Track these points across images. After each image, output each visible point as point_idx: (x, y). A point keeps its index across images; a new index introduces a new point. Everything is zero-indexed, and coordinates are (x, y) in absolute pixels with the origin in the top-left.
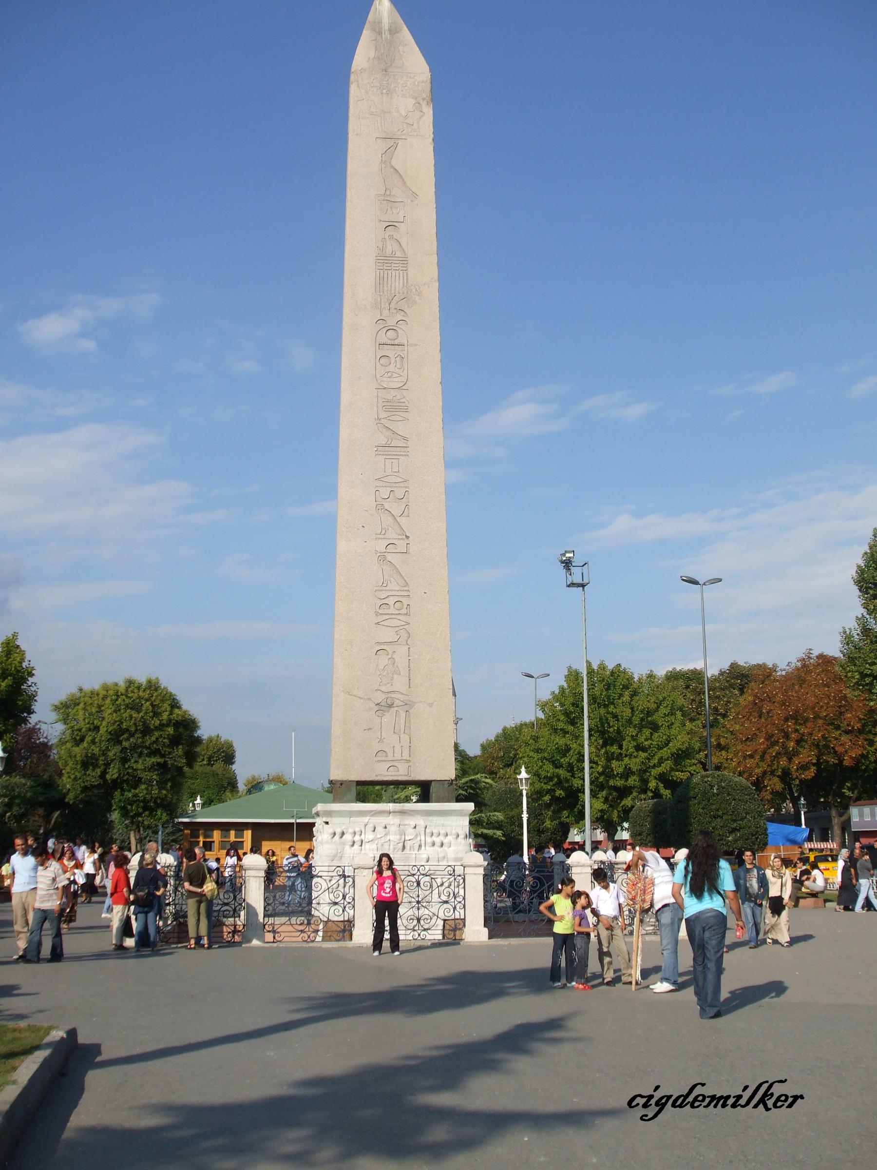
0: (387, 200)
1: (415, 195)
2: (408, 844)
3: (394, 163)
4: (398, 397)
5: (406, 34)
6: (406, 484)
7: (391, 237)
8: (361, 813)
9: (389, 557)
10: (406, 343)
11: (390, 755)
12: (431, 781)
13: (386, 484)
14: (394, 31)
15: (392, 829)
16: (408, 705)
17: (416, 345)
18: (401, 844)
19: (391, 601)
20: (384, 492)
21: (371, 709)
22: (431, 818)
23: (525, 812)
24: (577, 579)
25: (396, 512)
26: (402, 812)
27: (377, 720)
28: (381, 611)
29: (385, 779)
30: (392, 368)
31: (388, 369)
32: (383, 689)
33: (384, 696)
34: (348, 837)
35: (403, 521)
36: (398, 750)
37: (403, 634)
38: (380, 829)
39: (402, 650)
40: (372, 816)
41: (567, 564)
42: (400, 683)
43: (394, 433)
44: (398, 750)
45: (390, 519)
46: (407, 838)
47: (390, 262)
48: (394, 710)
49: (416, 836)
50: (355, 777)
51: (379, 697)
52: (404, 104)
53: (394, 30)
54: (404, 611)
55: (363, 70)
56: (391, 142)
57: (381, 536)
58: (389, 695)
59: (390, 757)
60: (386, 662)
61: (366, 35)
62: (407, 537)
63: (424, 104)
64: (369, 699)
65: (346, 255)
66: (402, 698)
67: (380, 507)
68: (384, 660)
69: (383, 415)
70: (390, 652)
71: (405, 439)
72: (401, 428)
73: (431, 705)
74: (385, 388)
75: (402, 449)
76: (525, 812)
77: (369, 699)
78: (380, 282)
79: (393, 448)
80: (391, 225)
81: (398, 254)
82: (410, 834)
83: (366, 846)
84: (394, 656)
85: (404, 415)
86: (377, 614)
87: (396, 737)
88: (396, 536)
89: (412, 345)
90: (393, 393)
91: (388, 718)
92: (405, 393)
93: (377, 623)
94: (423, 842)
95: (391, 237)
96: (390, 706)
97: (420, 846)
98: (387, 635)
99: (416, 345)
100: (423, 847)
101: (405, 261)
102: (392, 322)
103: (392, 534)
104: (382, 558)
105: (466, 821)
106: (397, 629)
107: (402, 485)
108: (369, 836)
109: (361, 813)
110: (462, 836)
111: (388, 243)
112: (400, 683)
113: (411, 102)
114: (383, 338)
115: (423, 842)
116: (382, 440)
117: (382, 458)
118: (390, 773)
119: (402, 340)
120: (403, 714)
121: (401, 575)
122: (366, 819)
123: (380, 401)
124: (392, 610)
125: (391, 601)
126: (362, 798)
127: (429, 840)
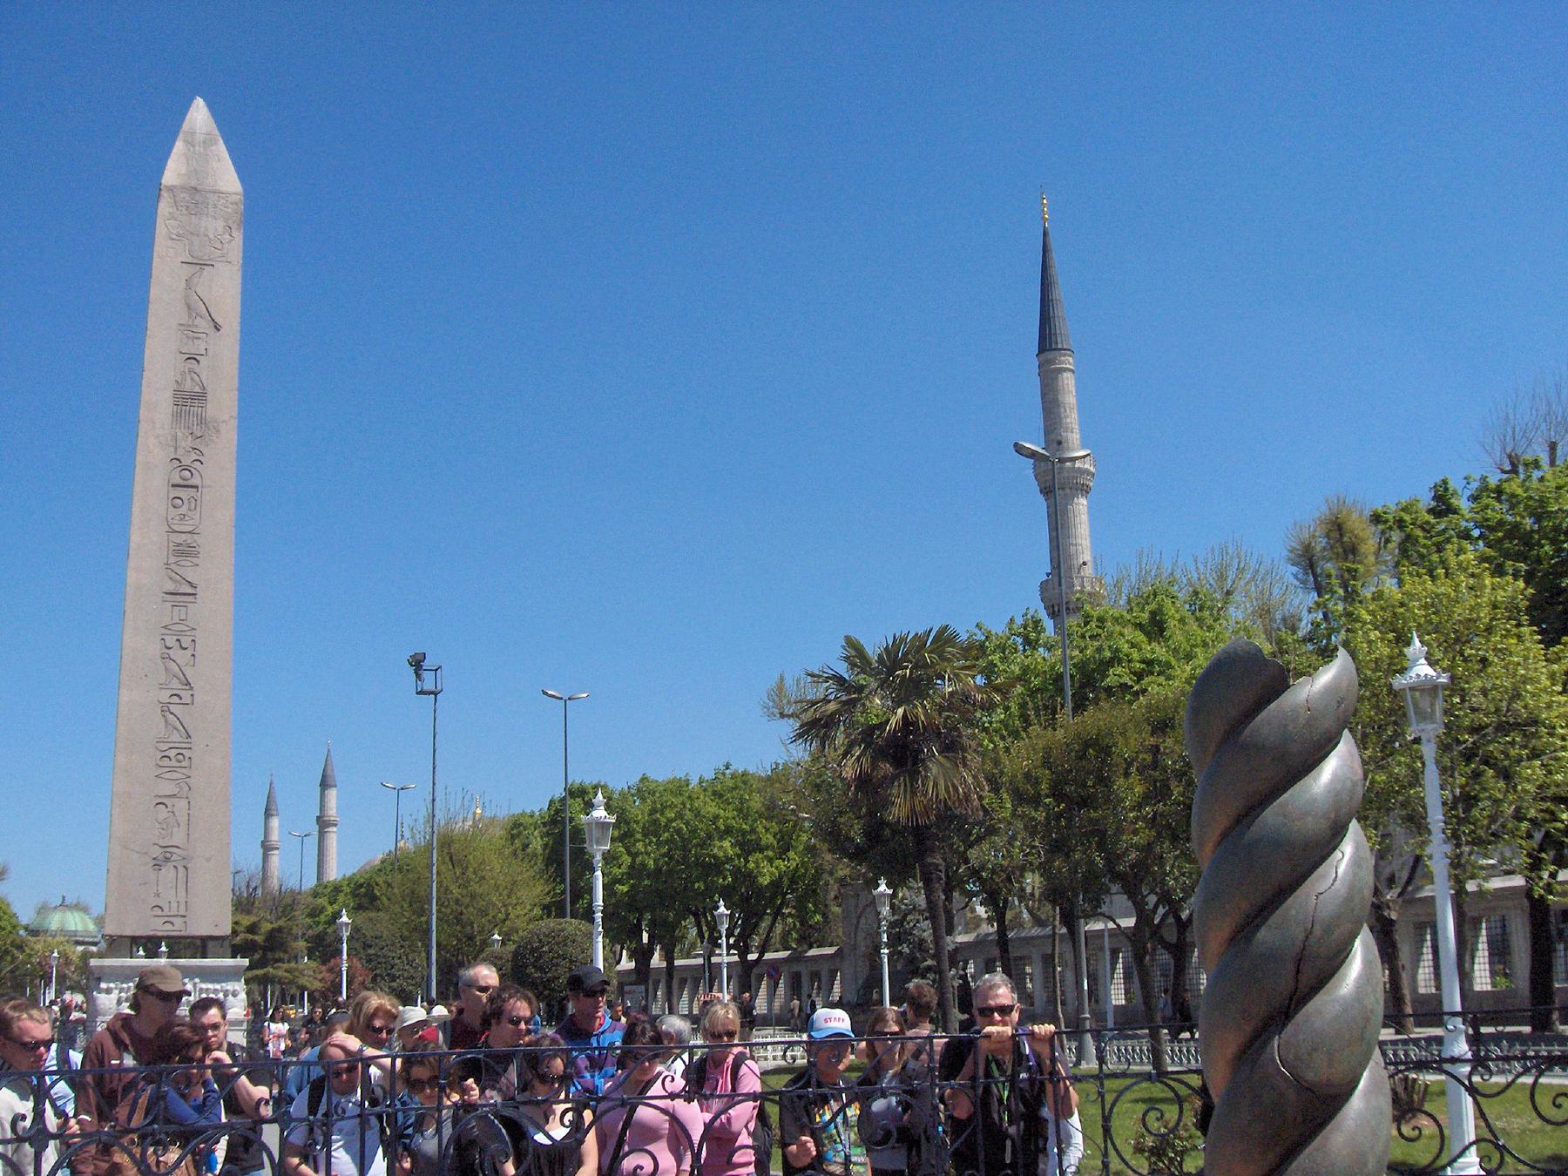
0: (189, 331)
1: (217, 328)
5: (221, 148)
7: (191, 371)
9: (172, 708)
14: (208, 142)
20: (171, 641)
24: (428, 685)
27: (152, 875)
30: (184, 510)
31: (181, 511)
35: (189, 672)
36: (174, 905)
39: (183, 803)
41: (417, 663)
42: (178, 838)
44: (174, 905)
47: (189, 401)
50: (128, 933)
51: (157, 852)
52: (213, 225)
53: (208, 142)
55: (171, 189)
59: (166, 912)
60: (165, 815)
61: (179, 146)
63: (234, 227)
69: (173, 559)
73: (208, 860)
79: (183, 594)
80: (192, 358)
81: (197, 389)
85: (195, 560)
91: (168, 872)
96: (167, 860)
98: (167, 788)
102: (186, 461)
103: (175, 684)
104: (165, 709)
113: (220, 224)
116: (170, 587)
119: (196, 481)
120: (181, 869)
125: (172, 753)
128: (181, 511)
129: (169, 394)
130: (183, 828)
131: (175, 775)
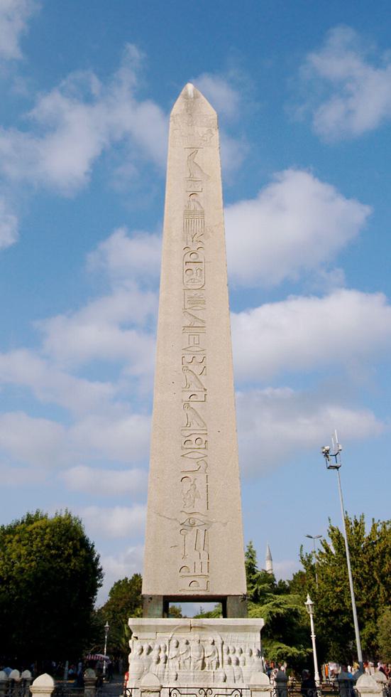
0: (191, 179)
3: (196, 160)
4: (199, 295)
6: (204, 352)
8: (166, 629)
9: (192, 405)
10: (203, 261)
11: (192, 570)
12: (226, 596)
13: (189, 352)
15: (193, 645)
16: (207, 524)
17: (210, 262)
18: (200, 662)
19: (193, 438)
21: (177, 528)
22: (226, 634)
23: (313, 633)
25: (197, 373)
28: (185, 446)
29: (188, 593)
32: (187, 510)
33: (187, 517)
34: (154, 654)
35: (202, 378)
36: (198, 566)
37: (202, 464)
38: (182, 645)
43: (196, 318)
44: (198, 566)
45: (193, 377)
48: (195, 529)
49: (214, 652)
51: (184, 518)
53: (196, 97)
54: (203, 446)
56: (194, 151)
57: (185, 389)
58: (192, 516)
61: (180, 99)
62: (205, 390)
64: (176, 519)
65: (165, 211)
66: (202, 518)
67: (185, 369)
68: (187, 485)
69: (188, 306)
70: (193, 480)
71: (203, 321)
72: (200, 315)
74: (189, 289)
75: (201, 328)
76: (313, 633)
77: (176, 519)
78: (186, 225)
82: (209, 649)
83: (170, 663)
84: (196, 483)
86: (182, 448)
87: (197, 553)
88: (197, 389)
89: (207, 262)
90: (195, 292)
91: (190, 536)
92: (203, 292)
93: (183, 456)
94: (220, 659)
95: (194, 200)
96: (192, 526)
97: (218, 664)
98: (191, 465)
99: (210, 262)
101: (202, 213)
102: (194, 249)
105: (257, 637)
106: (198, 460)
107: (201, 352)
108: (173, 653)
109: (166, 629)
110: (255, 654)
111: (192, 204)
112: (200, 506)
114: (188, 258)
115: (220, 659)
117: (187, 335)
118: (189, 588)
120: (202, 533)
121: (200, 418)
123: (186, 297)
124: (194, 446)
126: (166, 613)
127: (226, 658)
128: (192, 277)
129: (181, 213)
130: (203, 496)
131: (196, 455)
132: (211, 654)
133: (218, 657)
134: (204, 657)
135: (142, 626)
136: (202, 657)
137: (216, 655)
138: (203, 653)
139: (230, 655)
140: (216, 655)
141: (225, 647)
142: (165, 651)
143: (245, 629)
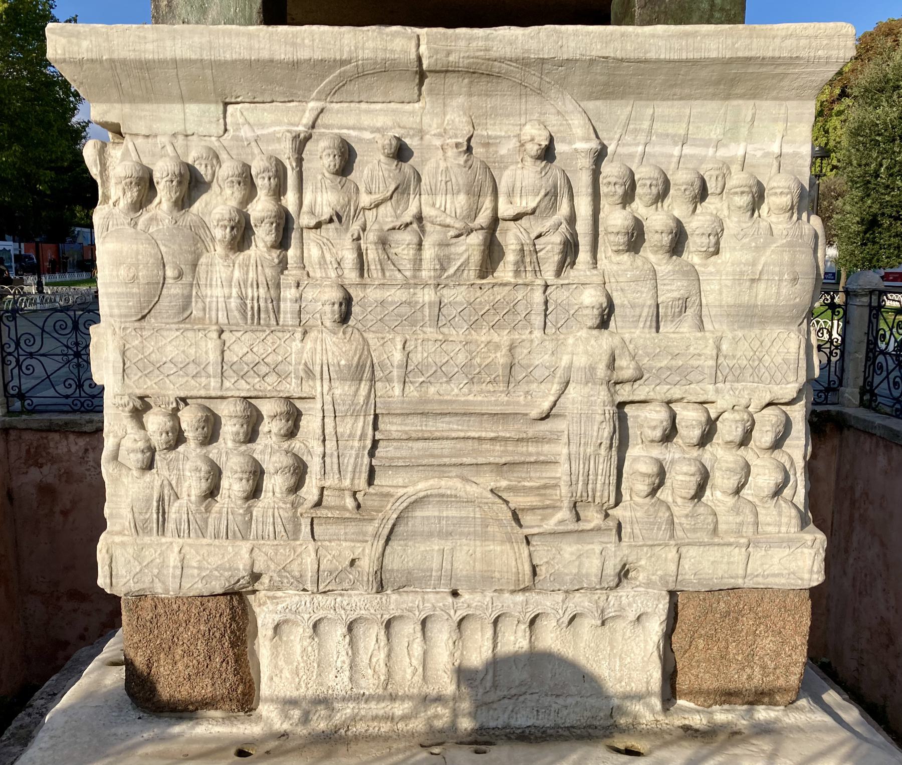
2: (511, 238)
15: (437, 163)
18: (476, 239)
26: (481, 73)
38: (373, 169)
40: (334, 92)
46: (505, 209)
49: (552, 195)
83: (310, 248)
94: (583, 227)
97: (570, 249)
100: (584, 255)
110: (779, 198)
115: (583, 227)
122: (300, 116)
127: (615, 219)
132: (531, 203)
133: (572, 220)
134: (495, 220)
135: (145, 67)
136: (483, 218)
137: (564, 209)
138: (487, 204)
139: (639, 207)
140: (564, 209)
141: (609, 169)
142: (279, 191)
143: (735, 80)
